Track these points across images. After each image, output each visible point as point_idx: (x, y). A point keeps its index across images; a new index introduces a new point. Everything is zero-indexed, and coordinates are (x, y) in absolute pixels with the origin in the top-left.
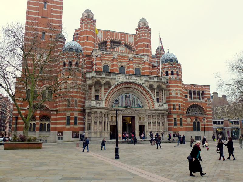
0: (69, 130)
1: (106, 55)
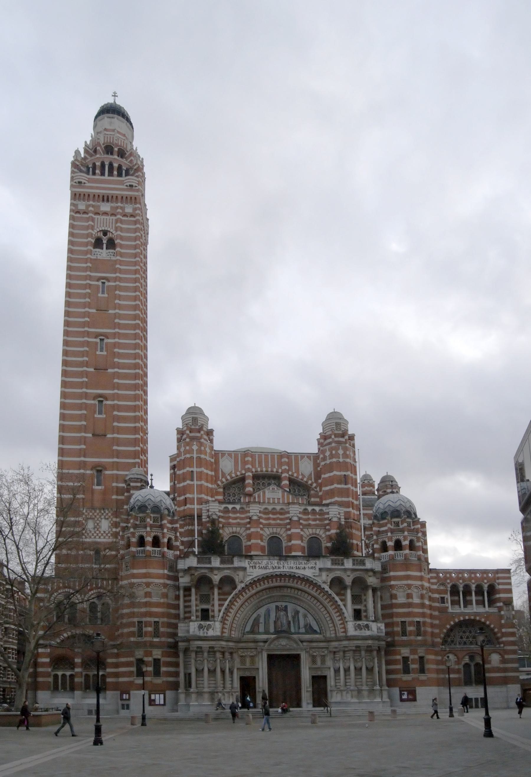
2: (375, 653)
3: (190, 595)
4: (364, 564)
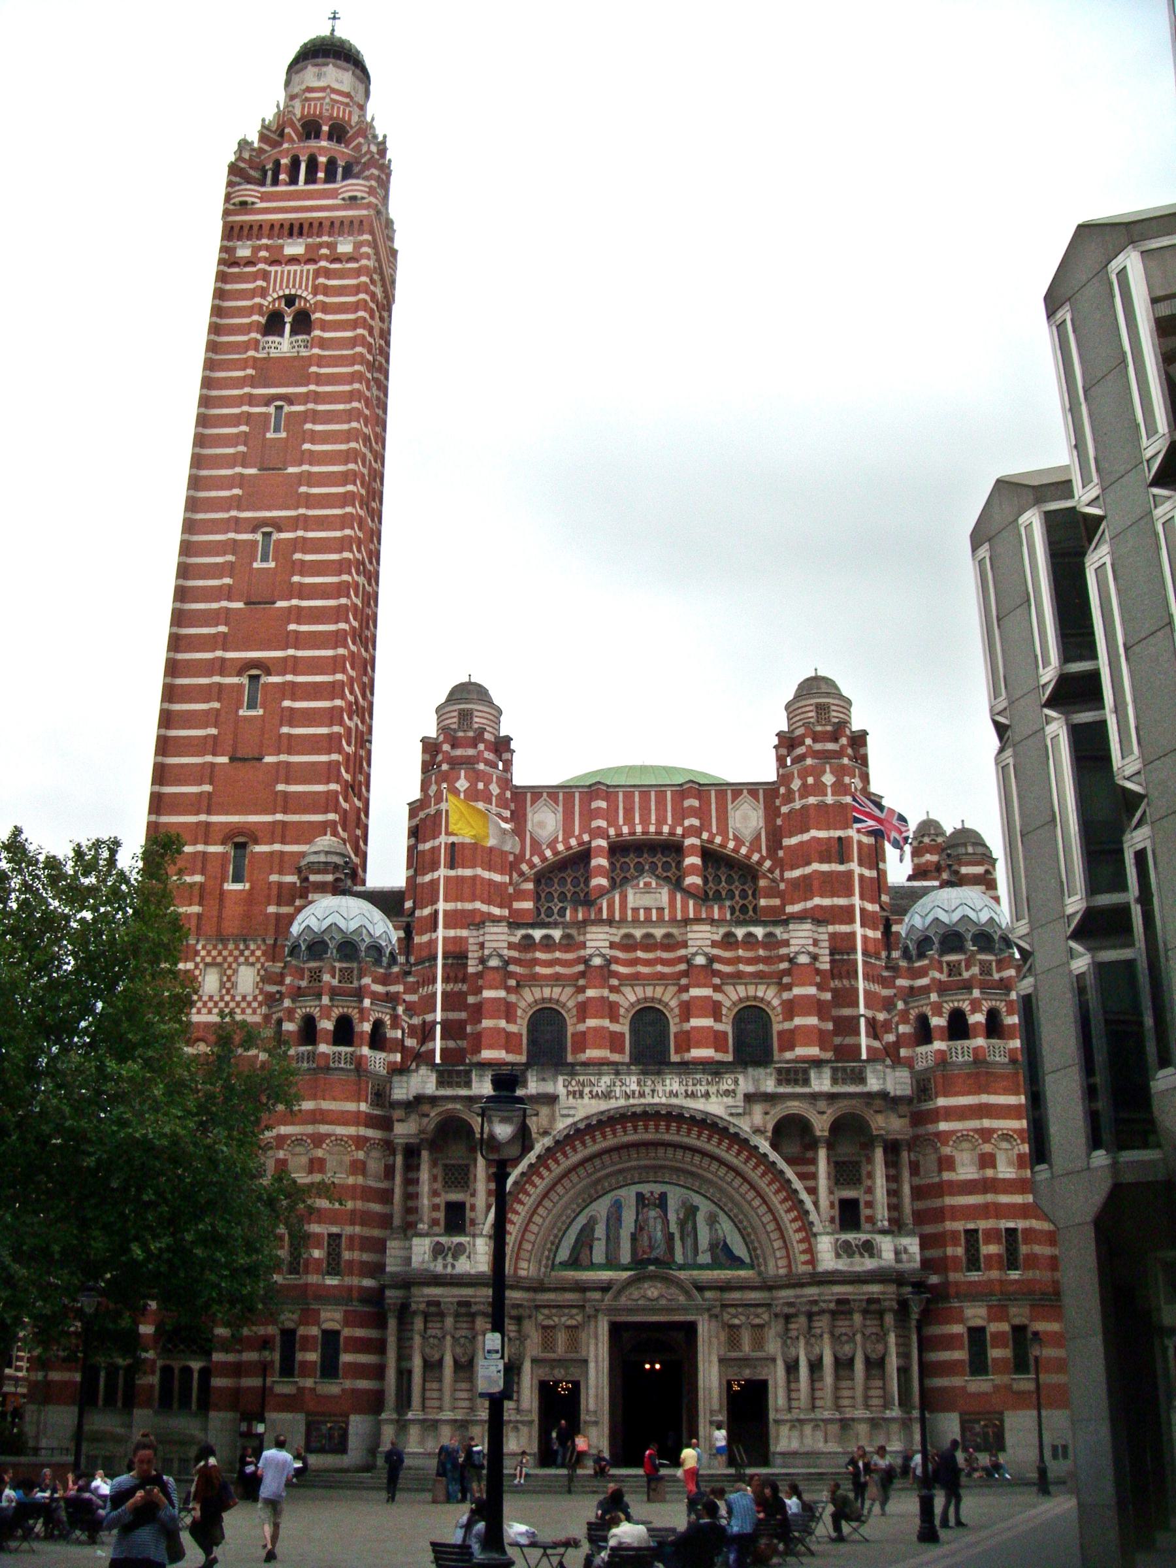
0: (291, 1403)
2: (889, 1319)
3: (417, 1168)
4: (862, 1080)
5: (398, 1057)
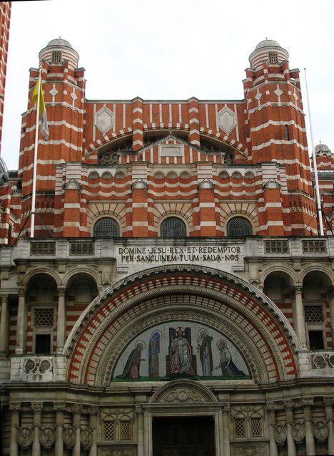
1: (107, 181)
3: (15, 313)
4: (324, 250)
5: (6, 241)
